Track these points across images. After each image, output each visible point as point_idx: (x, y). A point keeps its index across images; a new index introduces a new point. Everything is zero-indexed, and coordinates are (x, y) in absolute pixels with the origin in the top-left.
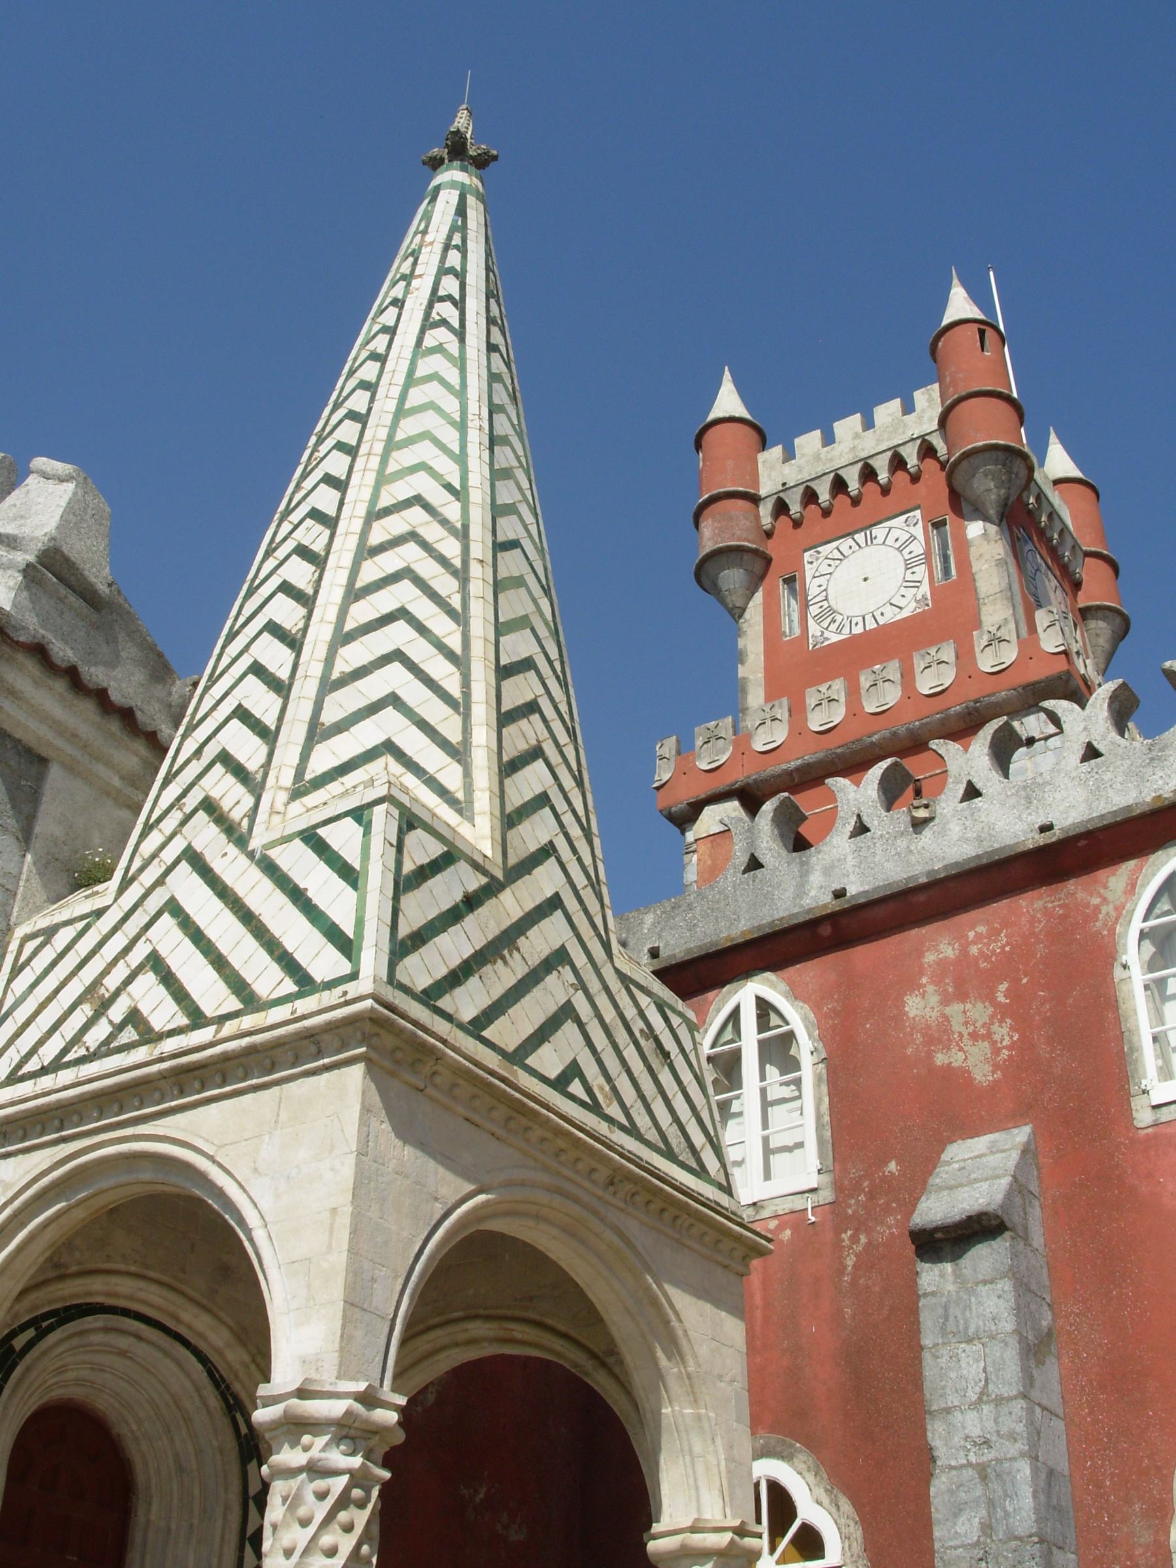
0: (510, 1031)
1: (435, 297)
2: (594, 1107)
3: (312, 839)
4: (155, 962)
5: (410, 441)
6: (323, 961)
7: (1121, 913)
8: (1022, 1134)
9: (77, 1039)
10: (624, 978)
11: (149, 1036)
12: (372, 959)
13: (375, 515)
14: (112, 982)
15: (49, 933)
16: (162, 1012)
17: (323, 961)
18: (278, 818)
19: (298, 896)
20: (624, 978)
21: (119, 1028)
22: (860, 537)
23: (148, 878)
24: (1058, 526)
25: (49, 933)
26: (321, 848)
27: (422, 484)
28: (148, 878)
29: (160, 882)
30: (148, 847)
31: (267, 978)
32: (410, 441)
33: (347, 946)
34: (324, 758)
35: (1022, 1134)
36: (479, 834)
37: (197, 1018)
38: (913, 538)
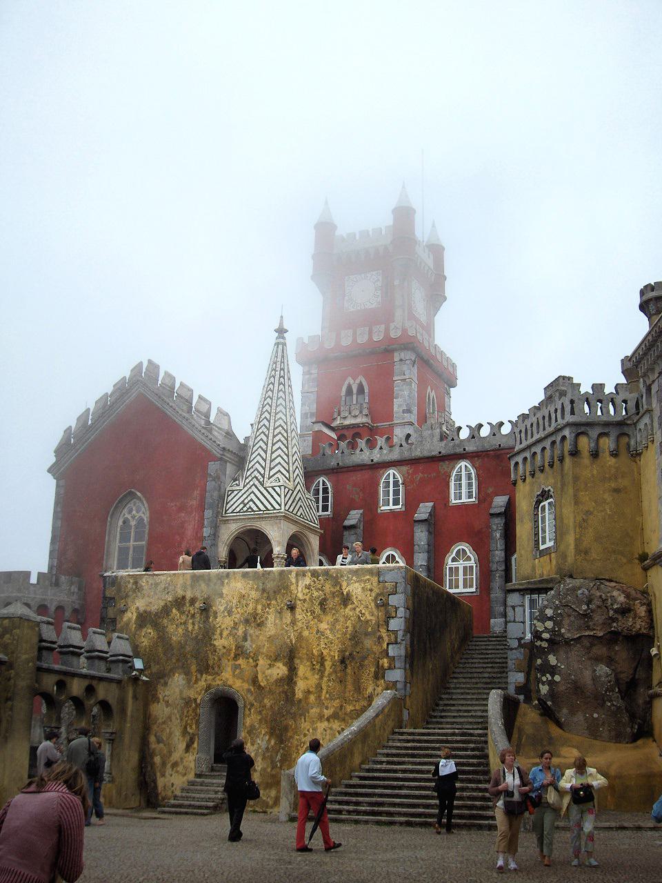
0: (295, 512)
1: (280, 377)
2: (303, 518)
3: (272, 487)
4: (252, 500)
5: (279, 412)
6: (277, 507)
7: (381, 477)
8: (361, 511)
9: (242, 509)
10: (307, 498)
11: (253, 511)
12: (283, 507)
13: (275, 429)
14: (246, 501)
15: (233, 491)
16: (255, 509)
17: (277, 507)
18: (267, 484)
19: (272, 496)
20: (307, 498)
21: (248, 509)
22: (363, 275)
23: (248, 486)
24: (426, 268)
25: (233, 491)
26: (274, 490)
27: (280, 422)
28: (248, 486)
29: (250, 488)
30: (247, 481)
31: (269, 507)
32: (279, 412)
33: (280, 505)
34: (271, 474)
35: (361, 511)
36: (291, 485)
37: (260, 510)
38: (378, 280)
